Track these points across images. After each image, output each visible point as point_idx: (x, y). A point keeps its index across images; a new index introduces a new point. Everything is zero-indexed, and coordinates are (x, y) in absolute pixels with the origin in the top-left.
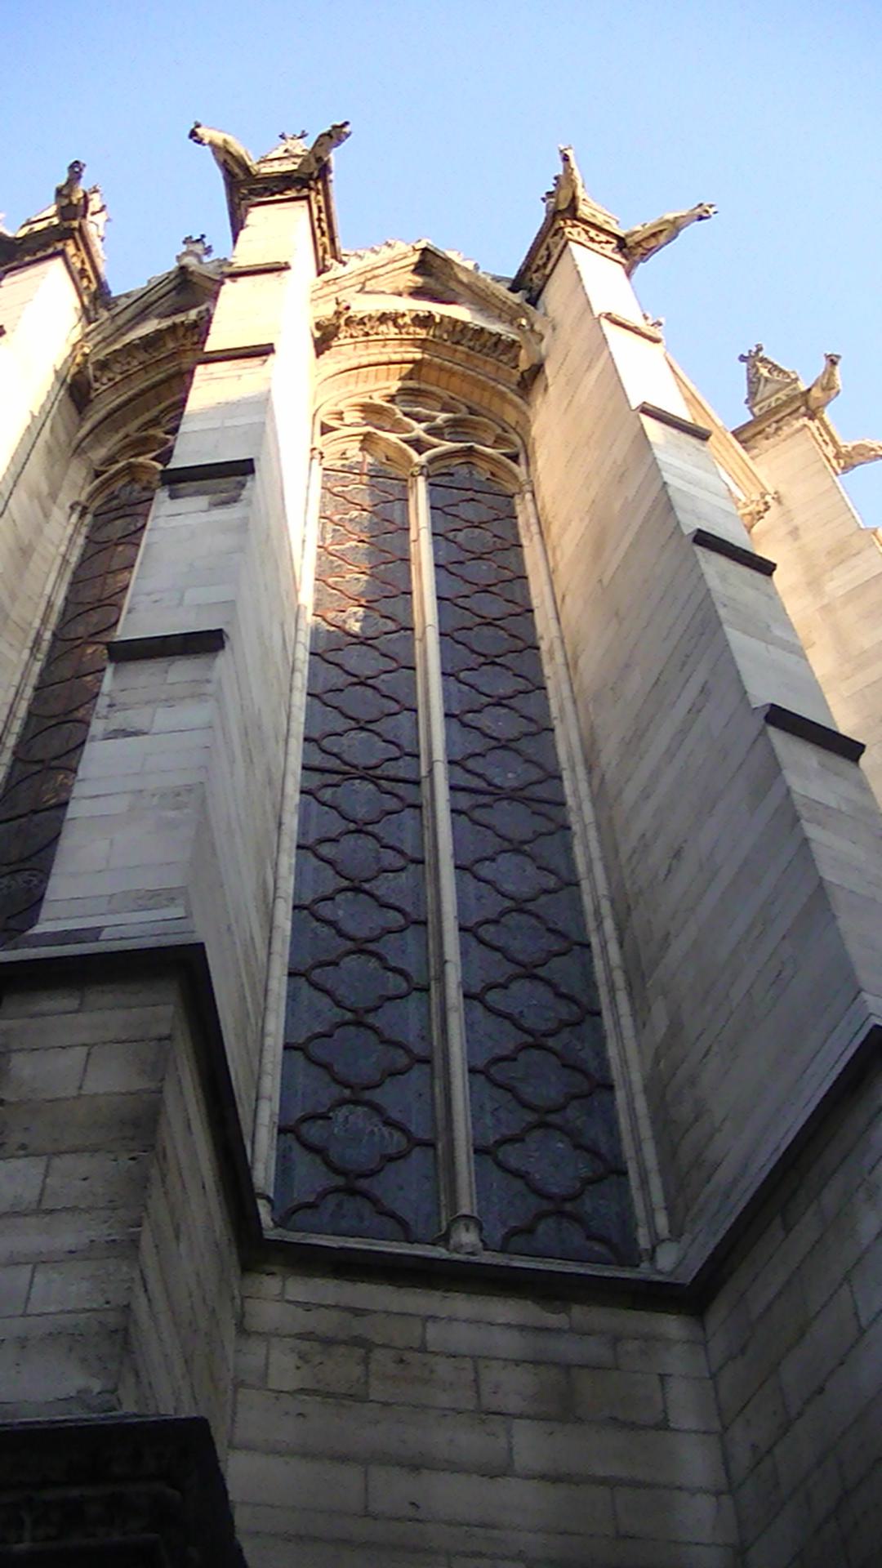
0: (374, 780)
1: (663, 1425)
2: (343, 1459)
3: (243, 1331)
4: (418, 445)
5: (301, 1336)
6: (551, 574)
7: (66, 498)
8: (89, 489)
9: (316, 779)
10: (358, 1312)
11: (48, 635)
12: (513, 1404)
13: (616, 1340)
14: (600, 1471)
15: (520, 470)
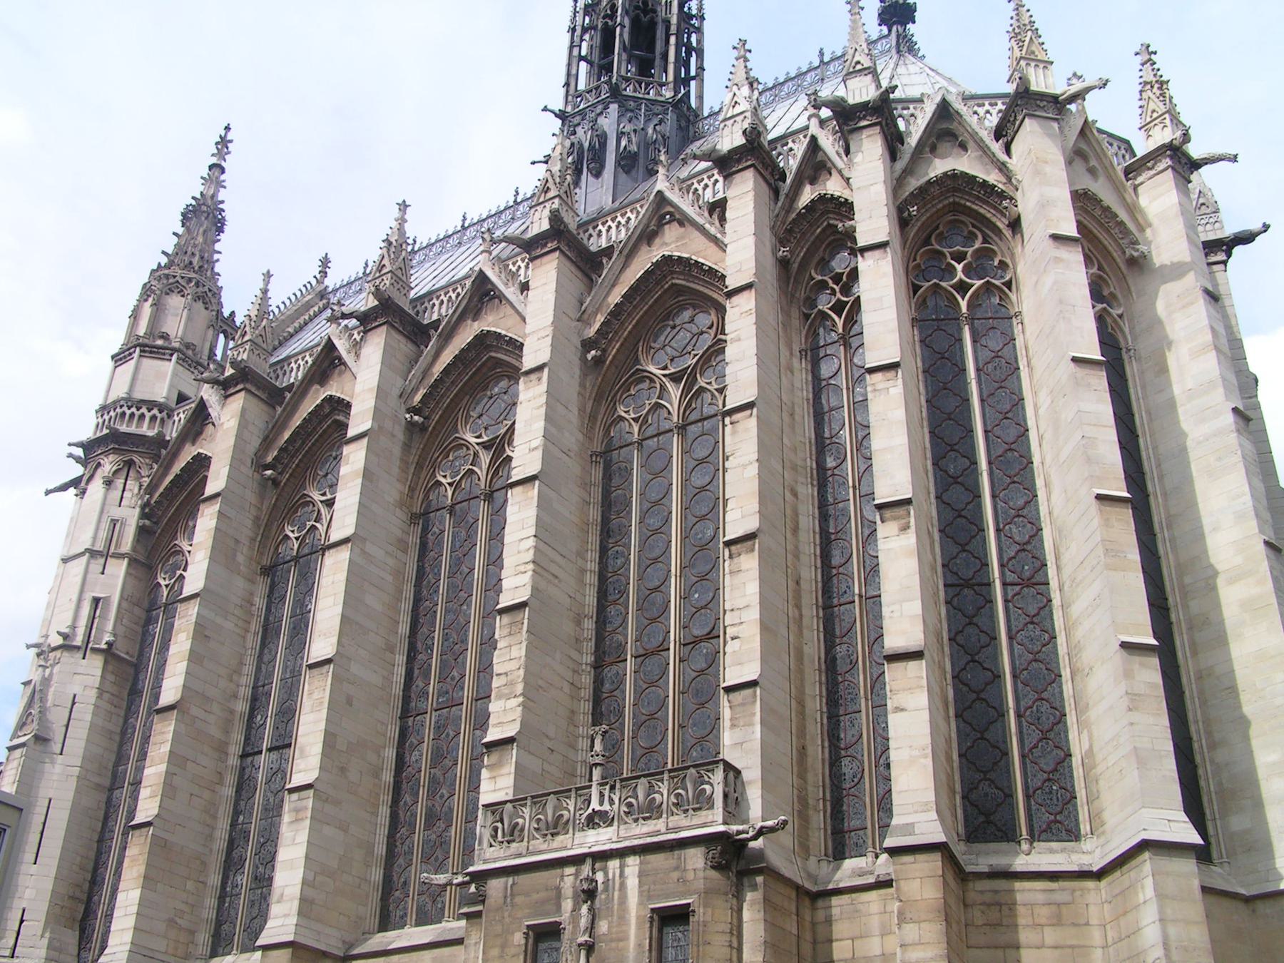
0: (971, 587)
1: (1087, 924)
2: (996, 947)
3: (966, 905)
4: (962, 288)
5: (983, 904)
6: (1035, 406)
7: (796, 349)
8: (804, 332)
9: (952, 591)
10: (996, 892)
11: (814, 466)
12: (1043, 921)
13: (1074, 891)
14: (1069, 943)
15: (1013, 296)
